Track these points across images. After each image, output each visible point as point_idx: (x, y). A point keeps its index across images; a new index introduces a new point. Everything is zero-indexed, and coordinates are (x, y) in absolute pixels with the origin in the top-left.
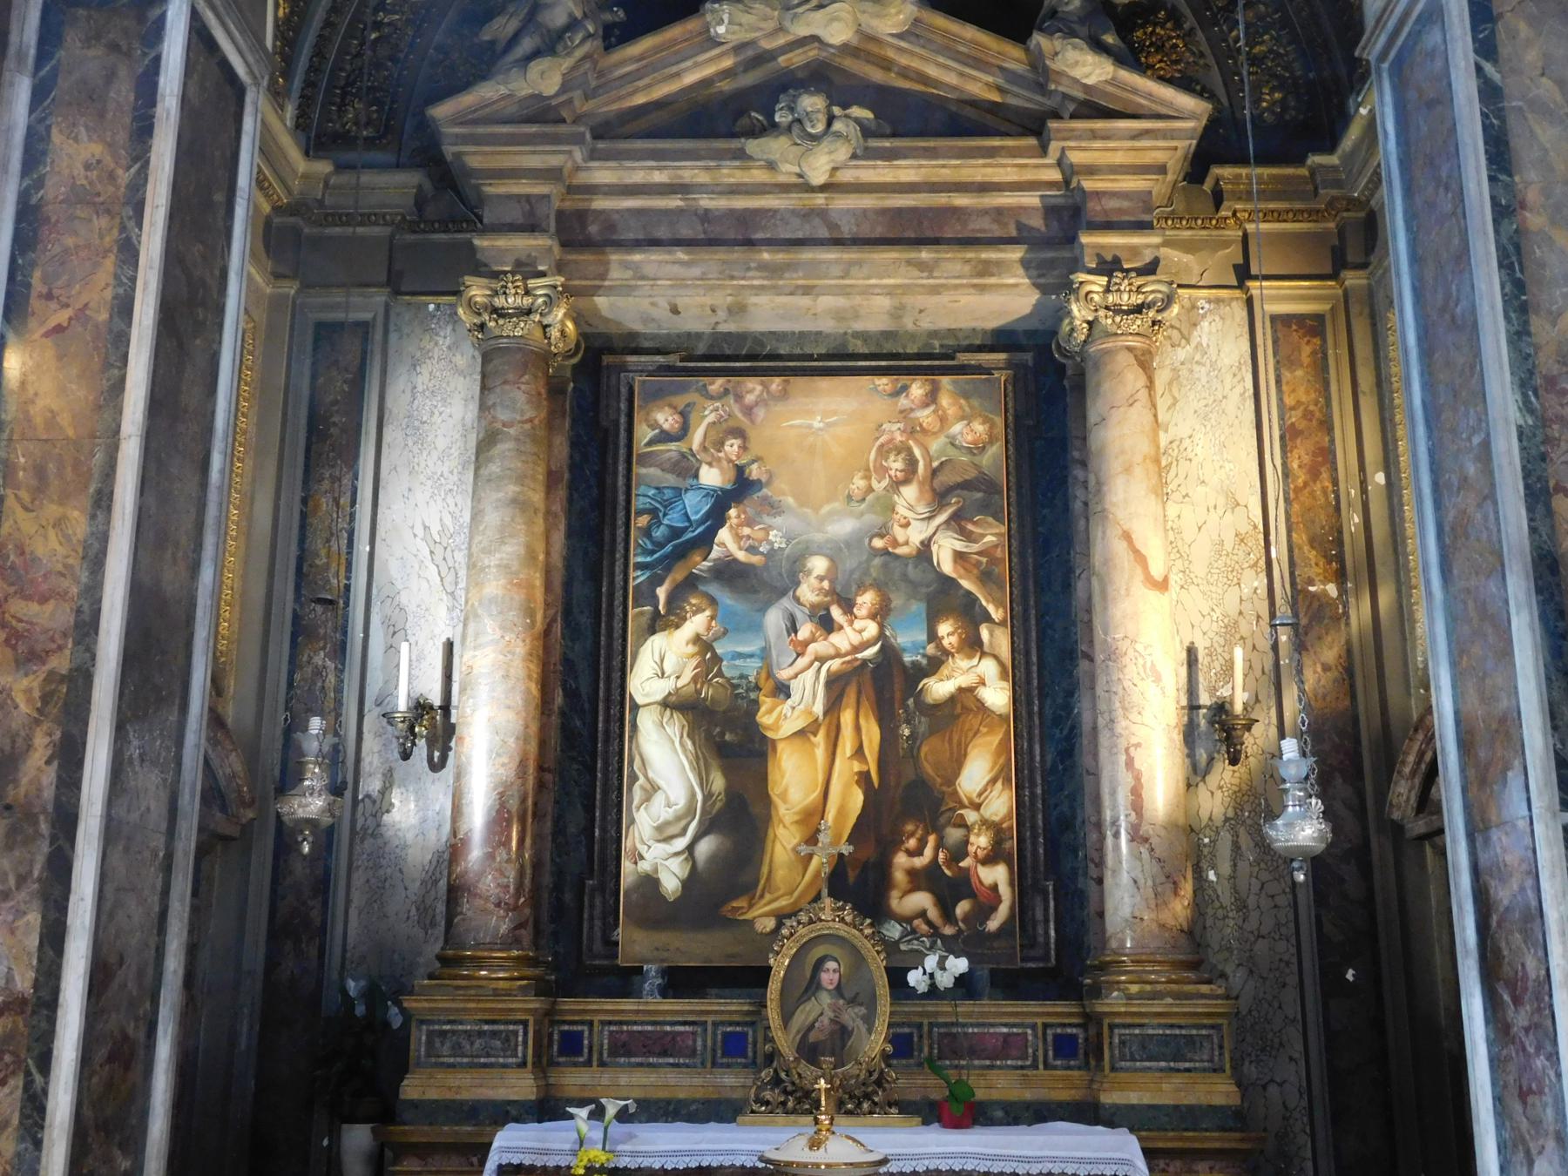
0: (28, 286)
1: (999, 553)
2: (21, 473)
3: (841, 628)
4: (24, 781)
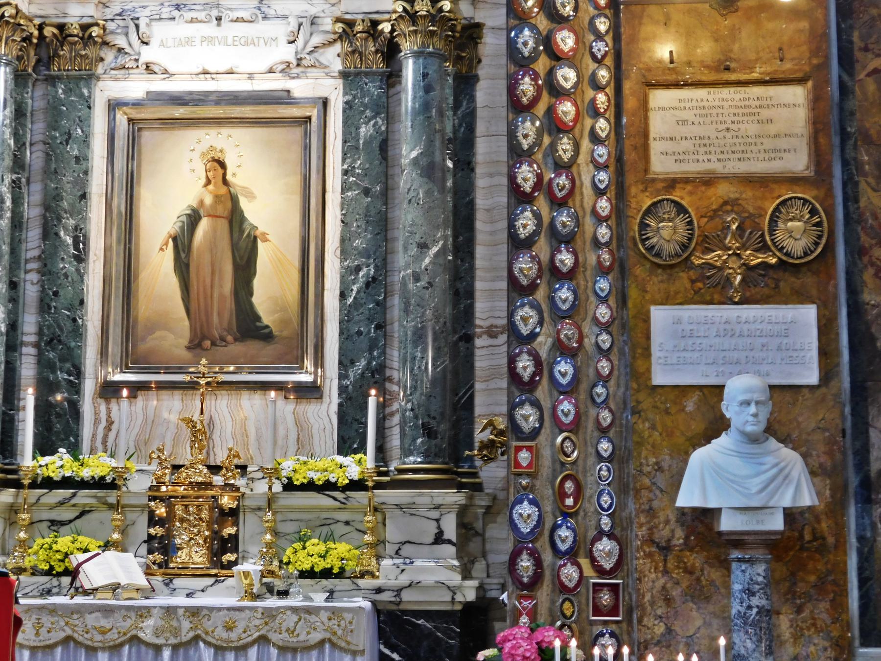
0: (851, 42)
2: (867, 167)
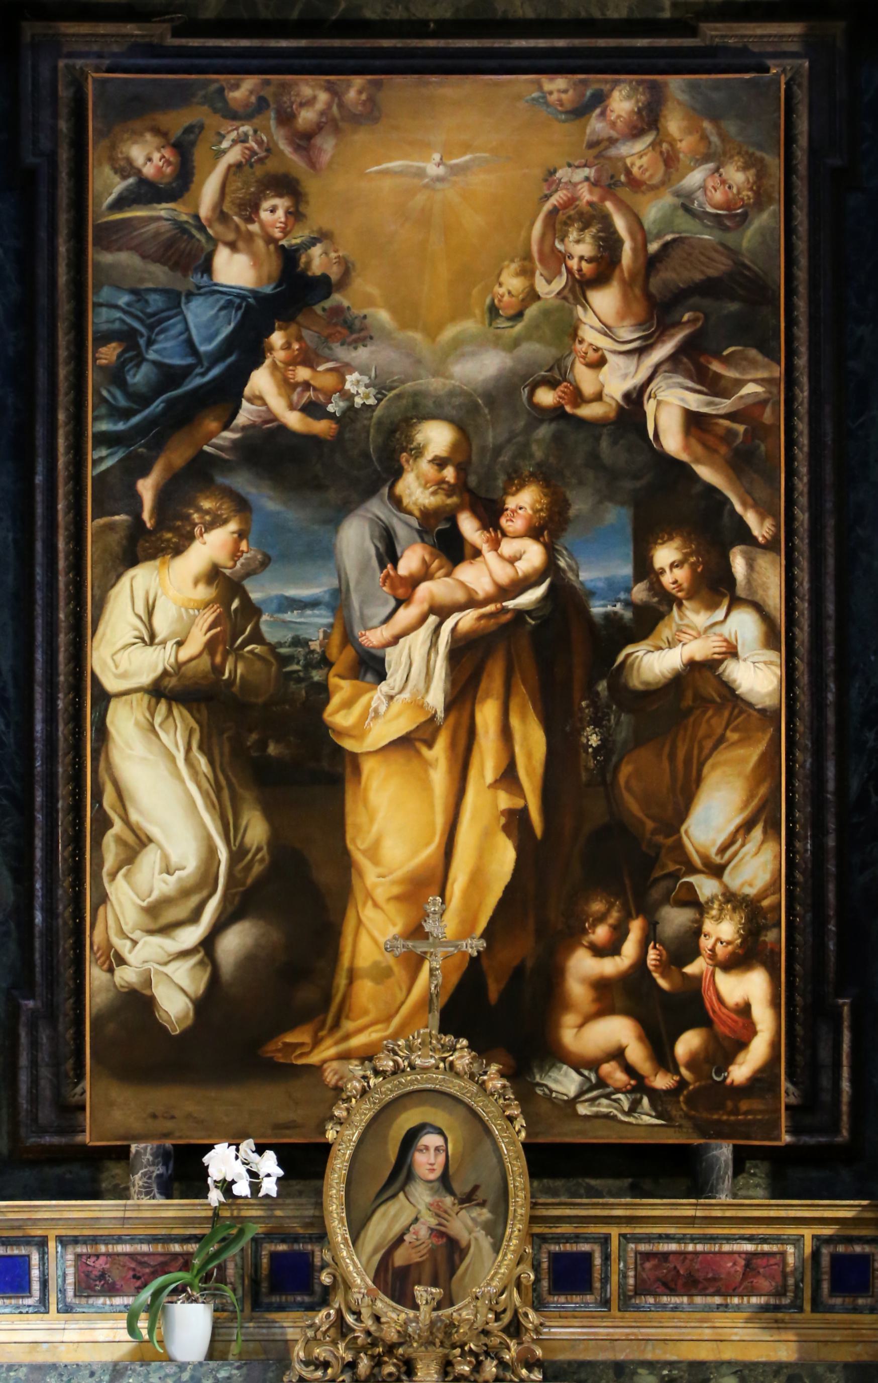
1: (767, 416)
3: (477, 553)
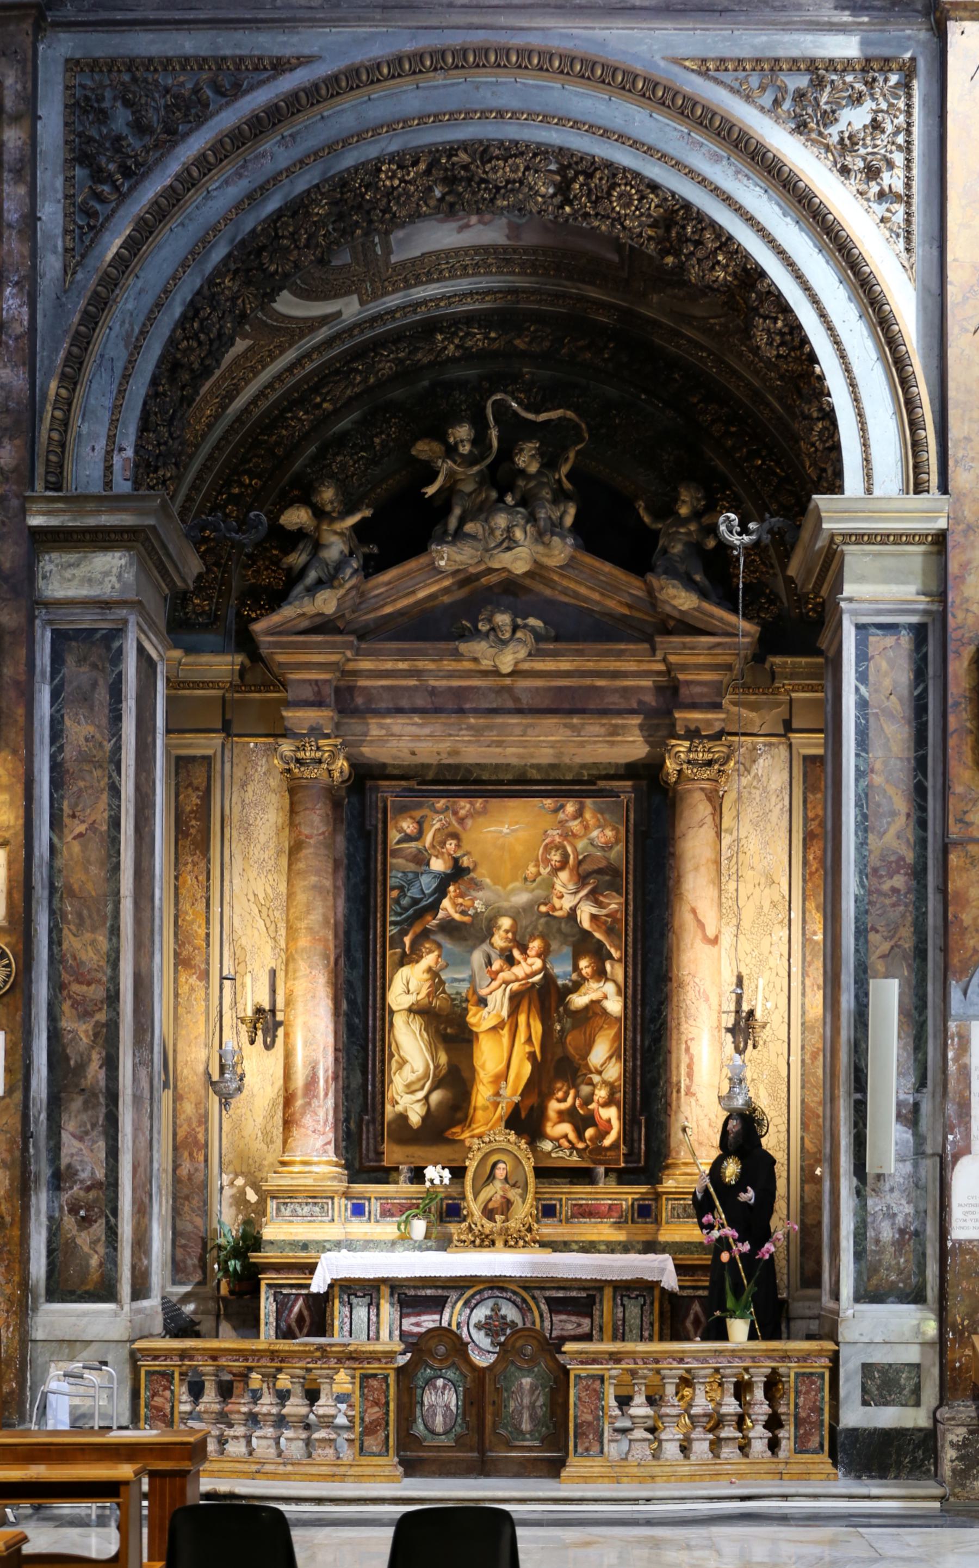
0: (61, 810)
1: (619, 916)
3: (519, 963)
4: (89, 1077)
